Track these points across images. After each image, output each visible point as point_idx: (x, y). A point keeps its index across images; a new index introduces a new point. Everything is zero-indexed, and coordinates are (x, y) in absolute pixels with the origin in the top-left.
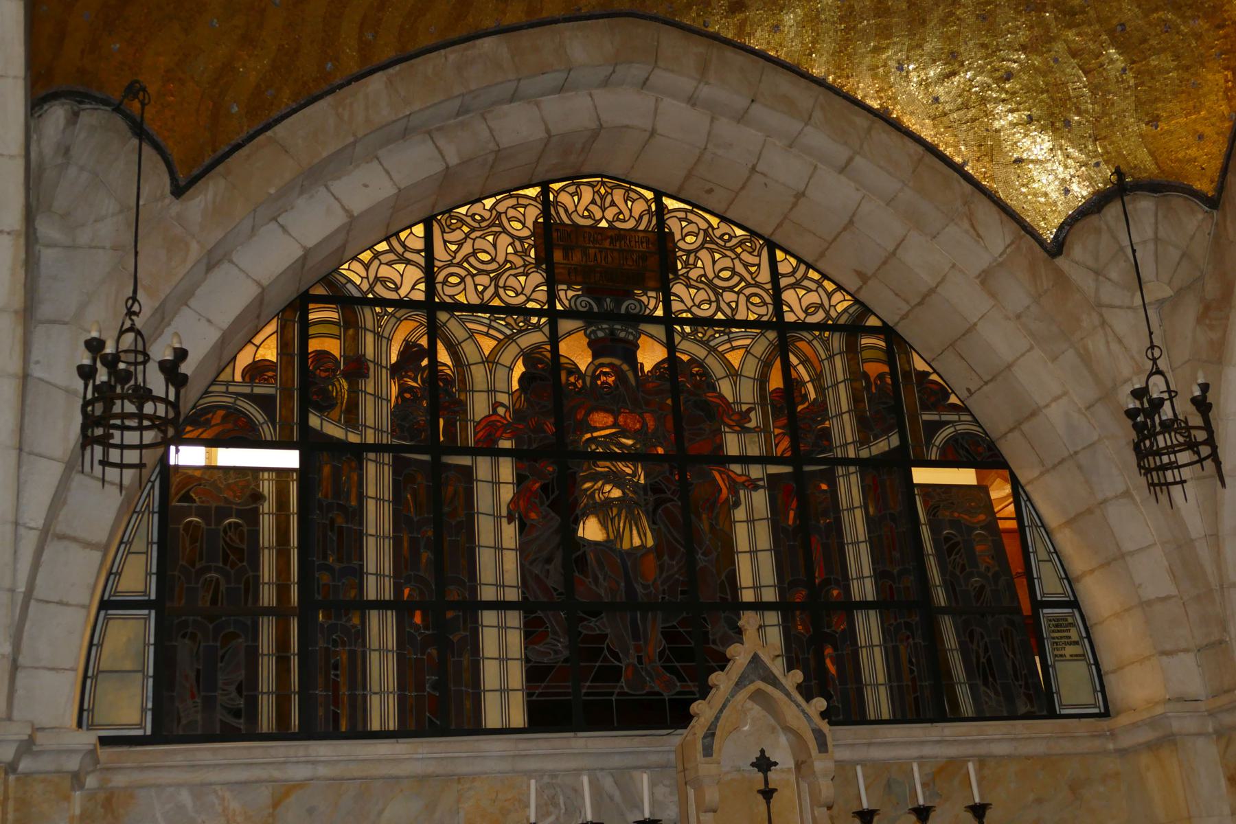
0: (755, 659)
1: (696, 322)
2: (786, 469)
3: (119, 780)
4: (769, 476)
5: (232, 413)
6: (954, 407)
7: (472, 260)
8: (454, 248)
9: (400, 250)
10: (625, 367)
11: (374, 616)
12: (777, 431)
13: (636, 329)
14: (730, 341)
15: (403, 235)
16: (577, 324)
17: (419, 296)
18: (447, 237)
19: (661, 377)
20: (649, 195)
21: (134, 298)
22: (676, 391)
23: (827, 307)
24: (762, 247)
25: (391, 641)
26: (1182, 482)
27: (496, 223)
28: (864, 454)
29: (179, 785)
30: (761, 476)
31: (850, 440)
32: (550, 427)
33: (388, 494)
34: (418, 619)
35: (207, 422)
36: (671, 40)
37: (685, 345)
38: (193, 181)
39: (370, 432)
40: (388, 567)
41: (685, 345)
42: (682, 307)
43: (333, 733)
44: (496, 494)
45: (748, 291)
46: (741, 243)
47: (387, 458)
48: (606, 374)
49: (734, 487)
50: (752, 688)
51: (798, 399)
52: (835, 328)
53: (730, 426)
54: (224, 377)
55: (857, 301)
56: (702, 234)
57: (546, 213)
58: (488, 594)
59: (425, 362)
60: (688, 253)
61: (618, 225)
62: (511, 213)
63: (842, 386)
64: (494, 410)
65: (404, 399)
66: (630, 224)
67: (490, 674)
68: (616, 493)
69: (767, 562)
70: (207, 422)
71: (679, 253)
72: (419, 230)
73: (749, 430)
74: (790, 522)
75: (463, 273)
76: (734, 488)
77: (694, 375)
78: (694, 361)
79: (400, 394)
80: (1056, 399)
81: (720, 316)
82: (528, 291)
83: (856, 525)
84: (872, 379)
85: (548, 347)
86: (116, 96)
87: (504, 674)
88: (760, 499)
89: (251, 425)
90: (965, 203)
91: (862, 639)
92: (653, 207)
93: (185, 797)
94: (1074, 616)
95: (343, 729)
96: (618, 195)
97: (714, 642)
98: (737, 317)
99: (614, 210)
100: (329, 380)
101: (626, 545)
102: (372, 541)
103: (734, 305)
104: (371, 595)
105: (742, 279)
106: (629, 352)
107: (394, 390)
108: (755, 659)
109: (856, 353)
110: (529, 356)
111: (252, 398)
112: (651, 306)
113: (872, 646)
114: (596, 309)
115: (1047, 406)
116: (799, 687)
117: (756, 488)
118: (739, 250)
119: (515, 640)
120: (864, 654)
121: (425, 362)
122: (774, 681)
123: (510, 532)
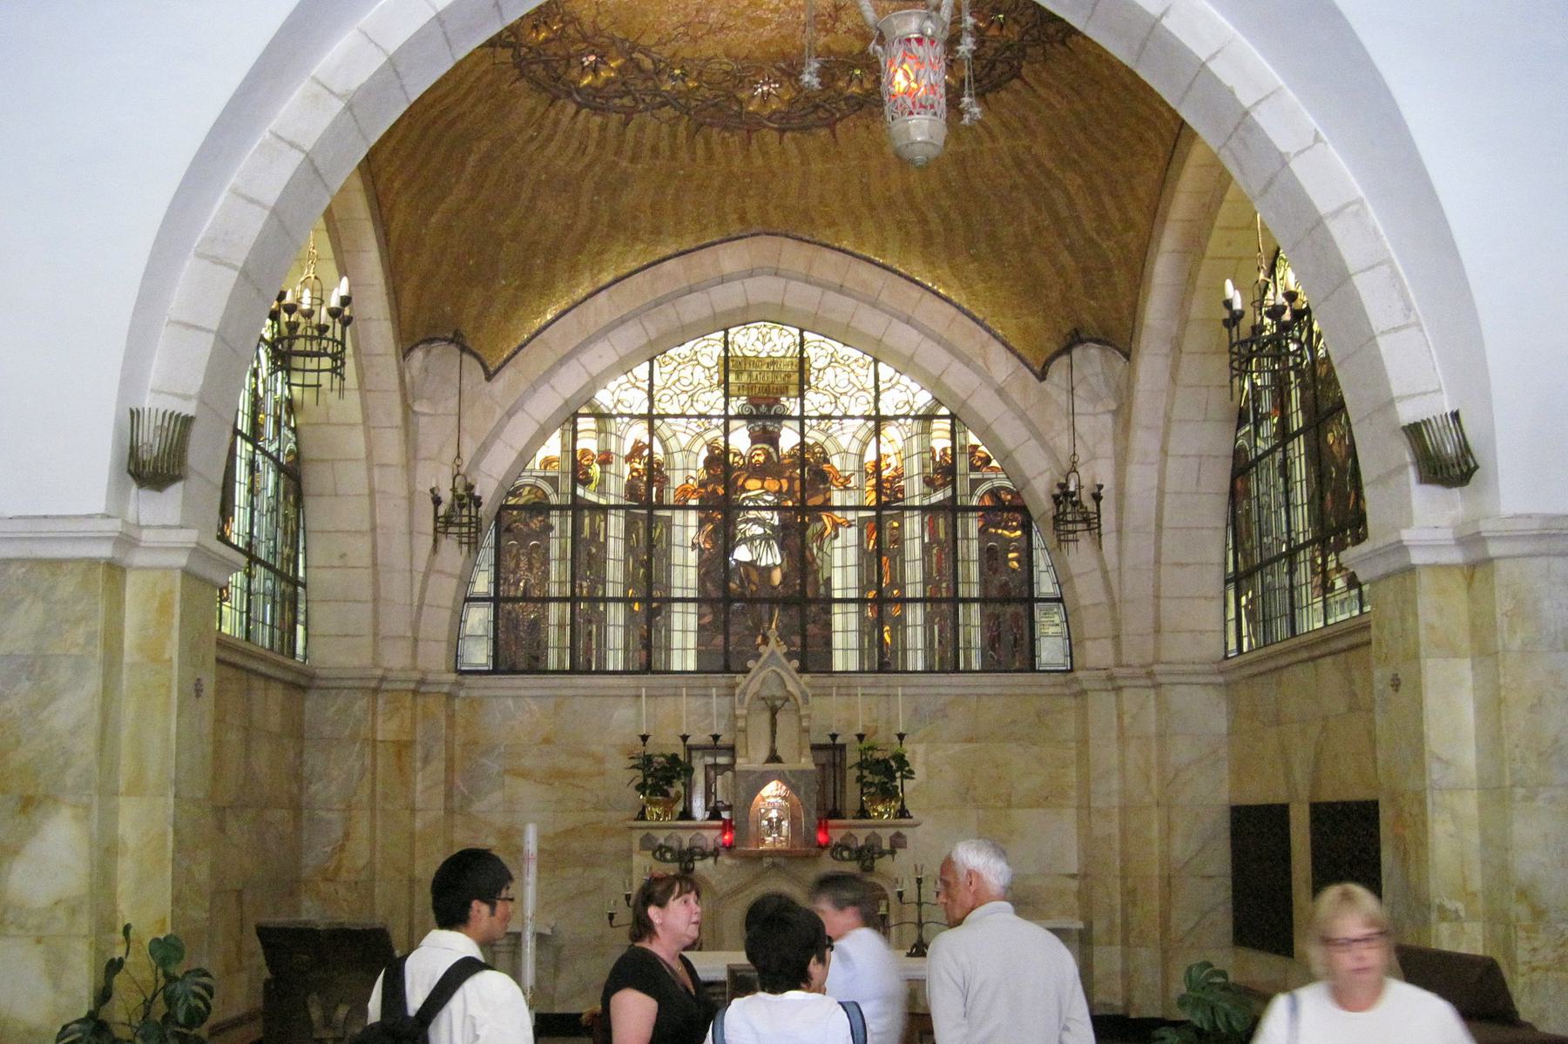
0: (772, 654)
1: (822, 417)
2: (874, 513)
3: (475, 693)
4: (859, 518)
5: (533, 486)
6: (993, 469)
7: (677, 384)
8: (665, 377)
9: (633, 380)
10: (771, 450)
11: (611, 606)
12: (867, 489)
13: (780, 423)
14: (842, 429)
15: (634, 371)
16: (743, 422)
17: (645, 411)
18: (663, 370)
19: (795, 455)
21: (458, 457)
22: (803, 463)
23: (911, 403)
24: (870, 363)
25: (621, 621)
26: (1077, 541)
27: (694, 360)
28: (926, 502)
29: (508, 697)
30: (853, 518)
31: (917, 493)
32: (721, 491)
33: (622, 535)
34: (636, 607)
36: (790, 245)
37: (811, 434)
39: (612, 497)
40: (620, 577)
41: (811, 434)
42: (812, 408)
43: (589, 672)
44: (684, 533)
45: (856, 395)
46: (856, 361)
47: (622, 513)
48: (758, 455)
49: (836, 526)
50: (770, 669)
51: (883, 465)
52: (916, 417)
53: (836, 486)
54: (528, 467)
55: (934, 398)
56: (829, 356)
57: (726, 349)
58: (677, 593)
60: (819, 370)
61: (773, 354)
62: (704, 351)
63: (915, 457)
64: (687, 482)
65: (633, 477)
66: (781, 353)
67: (677, 639)
68: (758, 530)
69: (852, 574)
71: (812, 371)
72: (647, 364)
73: (849, 489)
74: (870, 548)
75: (671, 393)
76: (836, 526)
77: (814, 453)
78: (816, 444)
79: (631, 473)
80: (1040, 474)
81: (837, 413)
82: (711, 404)
83: (914, 549)
84: (937, 452)
85: (723, 439)
86: (450, 336)
87: (685, 640)
88: (853, 532)
89: (546, 496)
90: (983, 347)
91: (910, 620)
92: (798, 341)
93: (510, 702)
94: (1059, 608)
95: (593, 669)
96: (775, 333)
97: (814, 622)
98: (848, 414)
99: (771, 344)
100: (589, 466)
101: (763, 564)
102: (611, 562)
103: (846, 405)
104: (611, 595)
105: (854, 385)
106: (773, 440)
107: (627, 469)
109: (930, 433)
111: (542, 478)
112: (791, 409)
113: (916, 626)
114: (755, 413)
115: (1035, 478)
117: (850, 526)
118: (854, 366)
119: (692, 621)
120: (910, 631)
121: (646, 452)
122: (782, 666)
123: (693, 557)
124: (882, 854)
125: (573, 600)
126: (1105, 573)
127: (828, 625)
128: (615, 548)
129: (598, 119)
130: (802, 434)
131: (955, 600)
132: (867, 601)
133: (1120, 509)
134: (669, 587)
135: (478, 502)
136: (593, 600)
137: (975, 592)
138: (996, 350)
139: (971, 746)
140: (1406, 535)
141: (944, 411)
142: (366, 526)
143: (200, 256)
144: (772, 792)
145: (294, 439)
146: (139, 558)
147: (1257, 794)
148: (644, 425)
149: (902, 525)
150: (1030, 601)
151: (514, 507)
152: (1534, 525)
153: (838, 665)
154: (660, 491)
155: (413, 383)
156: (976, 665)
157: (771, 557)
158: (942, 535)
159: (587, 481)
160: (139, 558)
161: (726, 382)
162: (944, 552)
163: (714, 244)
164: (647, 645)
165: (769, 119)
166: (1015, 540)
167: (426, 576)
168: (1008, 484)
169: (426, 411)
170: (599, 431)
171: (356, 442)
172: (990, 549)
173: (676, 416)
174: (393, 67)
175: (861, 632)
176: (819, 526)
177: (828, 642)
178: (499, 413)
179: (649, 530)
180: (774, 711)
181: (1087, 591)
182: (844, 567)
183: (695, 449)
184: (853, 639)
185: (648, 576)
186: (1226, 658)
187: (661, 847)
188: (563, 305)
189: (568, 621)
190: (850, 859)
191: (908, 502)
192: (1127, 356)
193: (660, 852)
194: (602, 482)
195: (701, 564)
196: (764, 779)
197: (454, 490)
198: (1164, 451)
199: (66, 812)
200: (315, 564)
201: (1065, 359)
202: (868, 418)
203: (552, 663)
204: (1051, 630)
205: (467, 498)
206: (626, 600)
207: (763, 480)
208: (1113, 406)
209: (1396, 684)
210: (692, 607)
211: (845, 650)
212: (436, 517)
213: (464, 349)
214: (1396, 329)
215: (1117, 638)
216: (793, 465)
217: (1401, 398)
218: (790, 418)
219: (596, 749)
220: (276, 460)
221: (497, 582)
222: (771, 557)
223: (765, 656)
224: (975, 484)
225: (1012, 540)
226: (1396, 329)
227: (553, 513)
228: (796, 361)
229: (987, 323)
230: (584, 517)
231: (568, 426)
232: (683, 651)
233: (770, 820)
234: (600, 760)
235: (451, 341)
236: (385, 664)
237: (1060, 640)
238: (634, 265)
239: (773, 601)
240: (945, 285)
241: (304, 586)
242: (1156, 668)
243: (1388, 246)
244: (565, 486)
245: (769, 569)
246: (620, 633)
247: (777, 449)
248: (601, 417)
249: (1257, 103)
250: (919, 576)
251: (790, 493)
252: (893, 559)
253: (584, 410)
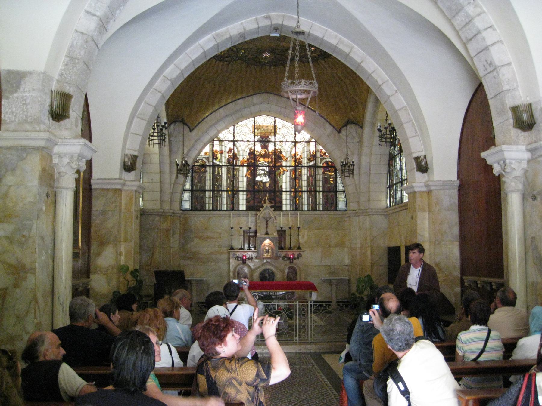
0: (267, 206)
1: (280, 142)
2: (294, 168)
5: (202, 160)
6: (326, 156)
11: (223, 193)
16: (259, 143)
20: (274, 118)
25: (226, 196)
28: (308, 165)
32: (253, 161)
33: (226, 173)
34: (230, 193)
35: (198, 162)
36: (272, 95)
38: (193, 129)
43: (217, 210)
47: (226, 167)
49: (284, 171)
51: (297, 155)
52: (306, 142)
54: (201, 154)
57: (254, 123)
58: (241, 189)
59: (232, 151)
63: (305, 153)
68: (262, 172)
69: (288, 184)
70: (198, 162)
72: (233, 127)
76: (284, 171)
83: (305, 177)
86: (180, 120)
87: (243, 202)
88: (288, 174)
89: (205, 163)
93: (195, 218)
101: (264, 181)
104: (223, 189)
106: (266, 147)
107: (227, 155)
108: (267, 206)
110: (250, 150)
116: (273, 210)
119: (245, 197)
120: (303, 200)
121: (232, 151)
122: (269, 209)
124: (295, 259)
125: (213, 191)
126: (356, 186)
127: (281, 198)
128: (224, 177)
129: (222, 63)
130: (275, 146)
131: (316, 191)
132: (292, 191)
133: (359, 168)
134: (239, 187)
135: (188, 165)
136: (218, 191)
137: (321, 189)
138: (327, 125)
139: (319, 231)
140: (414, 185)
141: (313, 140)
142: (158, 171)
143: (138, 117)
144: (267, 242)
146: (125, 188)
147: (393, 244)
148: (232, 143)
149: (302, 171)
150: (336, 191)
151: (197, 165)
152: (441, 183)
153: (284, 208)
154: (236, 161)
155: (171, 133)
156: (321, 209)
157: (266, 179)
158: (312, 174)
159: (216, 158)
160: (125, 188)
161: (254, 132)
162: (313, 178)
163: (252, 95)
164: (233, 203)
165: (267, 63)
166: (332, 175)
167: (174, 184)
168: (330, 160)
170: (220, 145)
172: (326, 178)
173: (241, 141)
174: (182, 73)
175: (290, 200)
176: (279, 171)
177: (281, 202)
178: (193, 141)
179: (233, 172)
180: (267, 222)
181: (351, 189)
182: (286, 182)
183: (246, 150)
184: (288, 202)
185: (233, 183)
186: (387, 207)
187: (237, 257)
188: (211, 112)
189: (211, 196)
190: (287, 260)
191: (303, 165)
192: (362, 127)
193: (237, 258)
194: (221, 159)
195: (247, 181)
196: (265, 239)
197: (182, 162)
198: (371, 152)
199: (111, 245)
201: (345, 127)
202: (293, 142)
203: (207, 208)
204: (342, 200)
205: (187, 164)
206: (227, 191)
207: (264, 159)
208: (358, 140)
209: (412, 218)
210: (245, 193)
211: (286, 204)
212: (178, 170)
213: (185, 124)
214: (413, 137)
215: (358, 202)
216: (272, 155)
217: (413, 153)
218: (271, 142)
219: (219, 231)
221: (192, 185)
222: (266, 179)
223: (265, 207)
224: (321, 160)
225: (331, 175)
226: (413, 137)
227: (207, 167)
228: (273, 126)
229: (325, 117)
230: (215, 168)
231: (211, 143)
232: (242, 204)
233: (266, 250)
234: (220, 234)
235: (181, 122)
236: (164, 208)
237: (344, 202)
238: (229, 101)
239: (266, 191)
240: (314, 107)
242: (369, 210)
243: (412, 117)
244: (211, 159)
245: (265, 183)
246: (225, 200)
247: (268, 151)
248: (220, 141)
249: (382, 84)
250: (306, 185)
251: (272, 162)
252: (299, 180)
253: (215, 139)
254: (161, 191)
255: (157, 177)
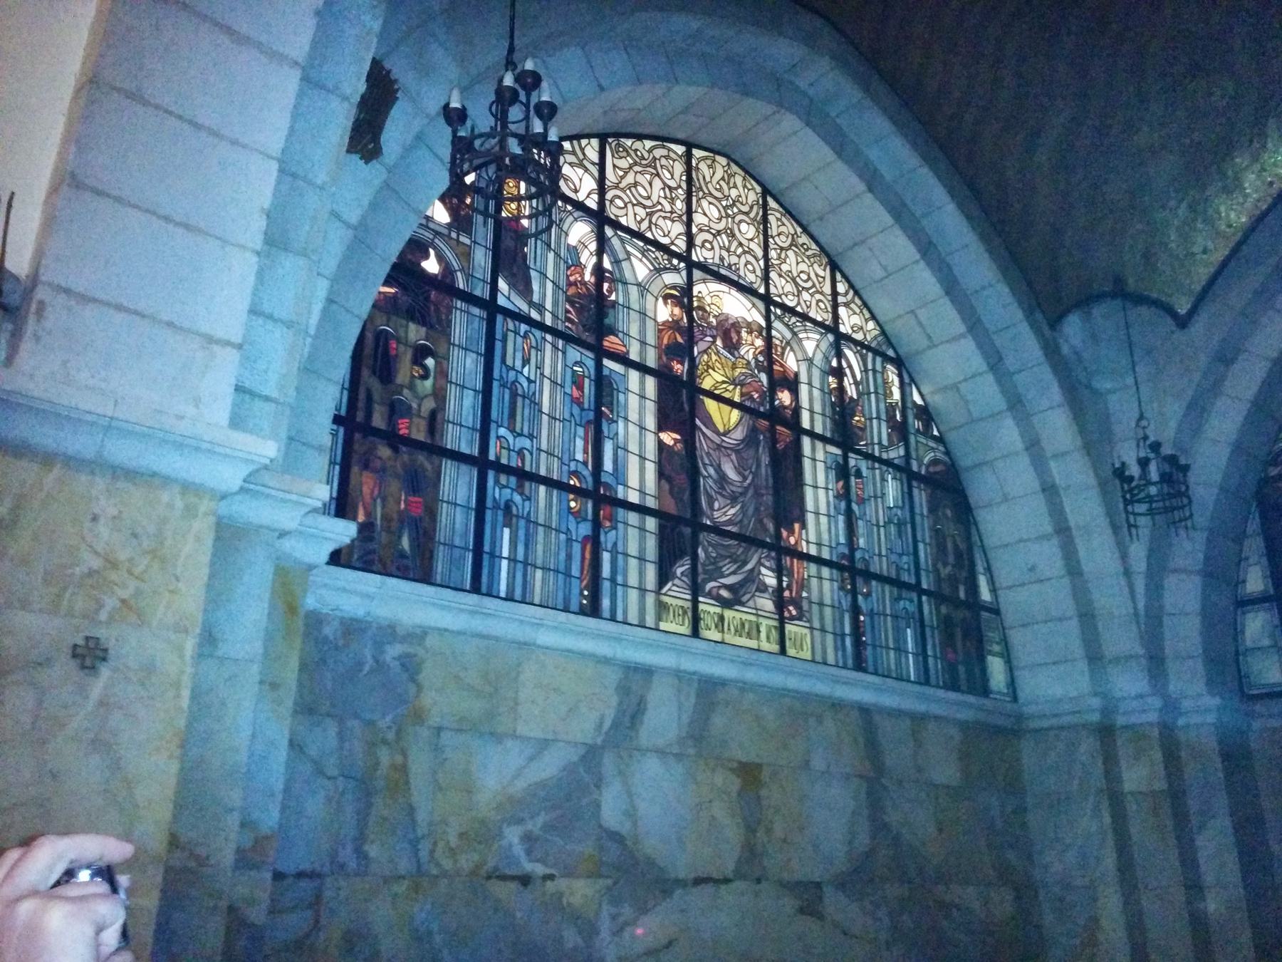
142: (1049, 529)
145: (941, 448)
169: (1108, 386)
171: (1009, 434)
200: (1004, 585)
213: (1141, 300)
220: (904, 471)
235: (1114, 295)
241: (996, 611)
254: (1087, 617)
255: (1048, 557)
